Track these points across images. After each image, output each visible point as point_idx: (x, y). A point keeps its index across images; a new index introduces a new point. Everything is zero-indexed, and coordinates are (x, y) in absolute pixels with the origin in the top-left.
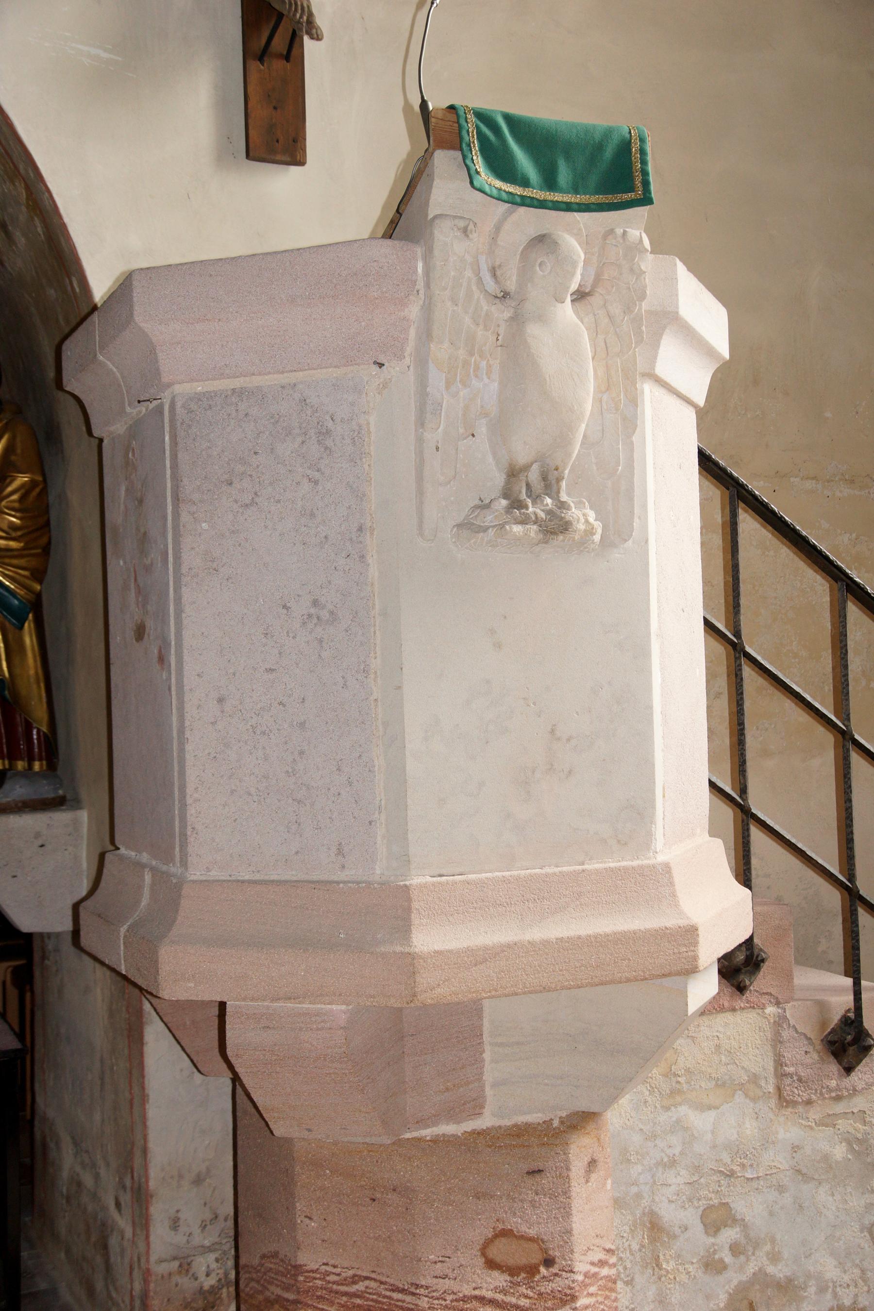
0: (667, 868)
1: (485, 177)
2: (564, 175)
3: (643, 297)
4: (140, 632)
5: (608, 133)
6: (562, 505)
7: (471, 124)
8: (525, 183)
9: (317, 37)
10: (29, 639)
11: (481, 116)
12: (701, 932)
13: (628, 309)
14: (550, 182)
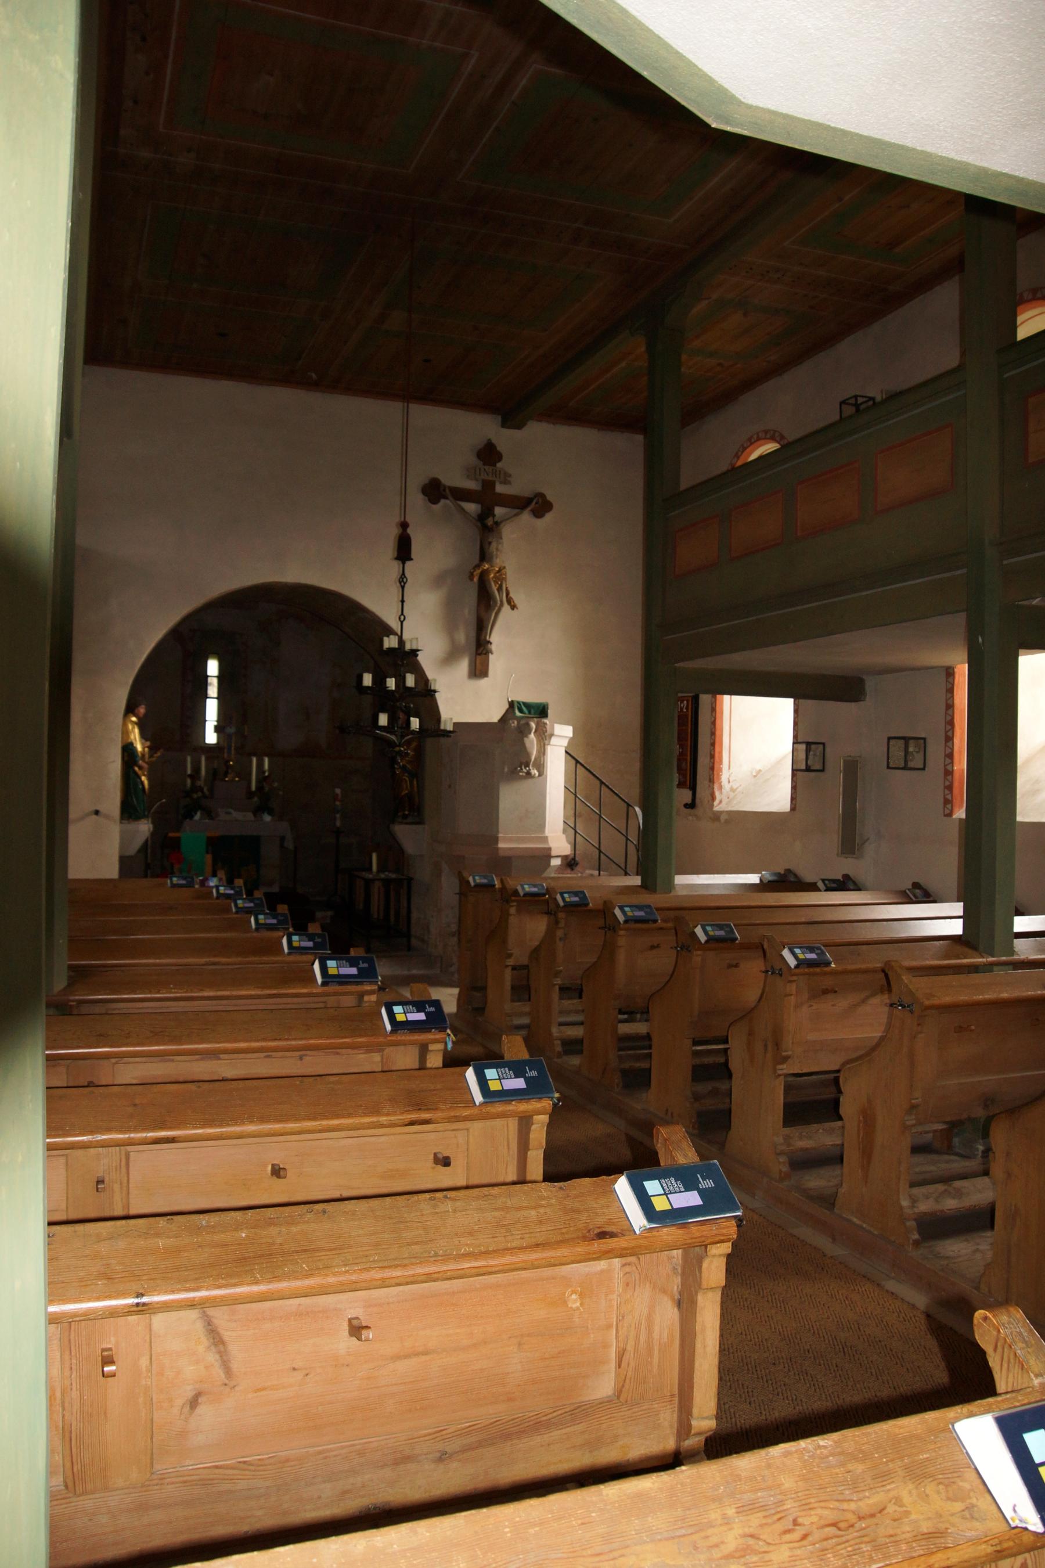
0: (547, 837)
1: (518, 714)
2: (532, 711)
3: (546, 731)
4: (450, 786)
5: (541, 704)
6: (530, 770)
7: (516, 705)
8: (525, 713)
9: (492, 654)
10: (415, 783)
11: (518, 703)
12: (553, 849)
13: (544, 734)
14: (530, 713)
